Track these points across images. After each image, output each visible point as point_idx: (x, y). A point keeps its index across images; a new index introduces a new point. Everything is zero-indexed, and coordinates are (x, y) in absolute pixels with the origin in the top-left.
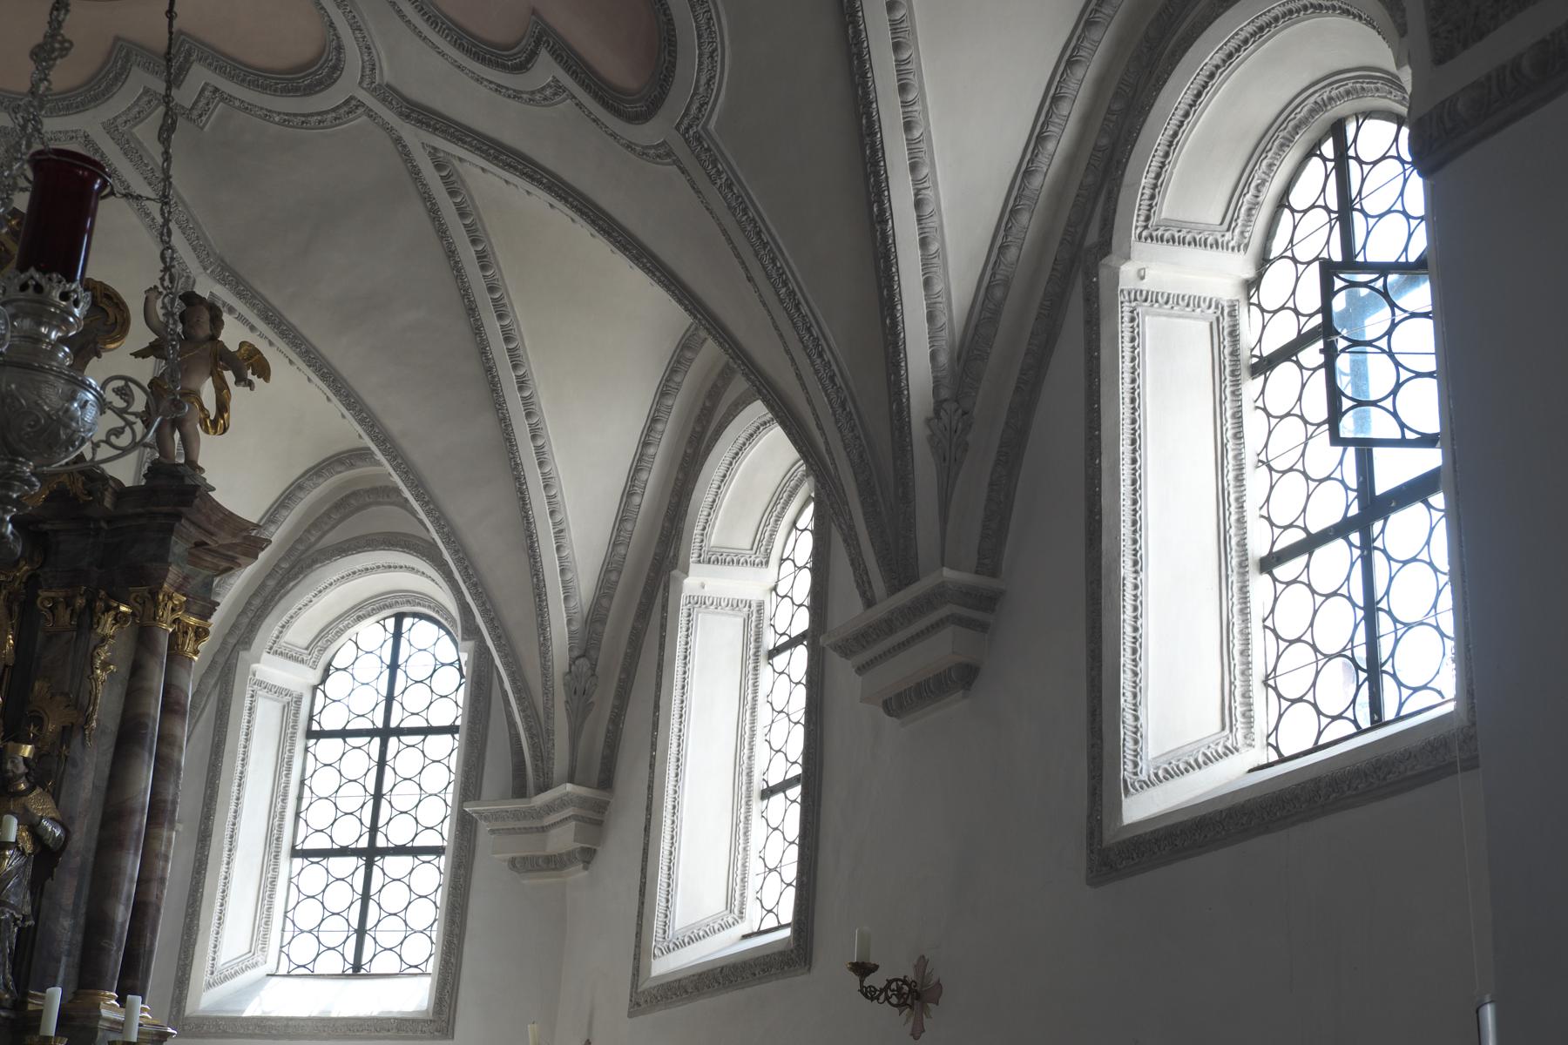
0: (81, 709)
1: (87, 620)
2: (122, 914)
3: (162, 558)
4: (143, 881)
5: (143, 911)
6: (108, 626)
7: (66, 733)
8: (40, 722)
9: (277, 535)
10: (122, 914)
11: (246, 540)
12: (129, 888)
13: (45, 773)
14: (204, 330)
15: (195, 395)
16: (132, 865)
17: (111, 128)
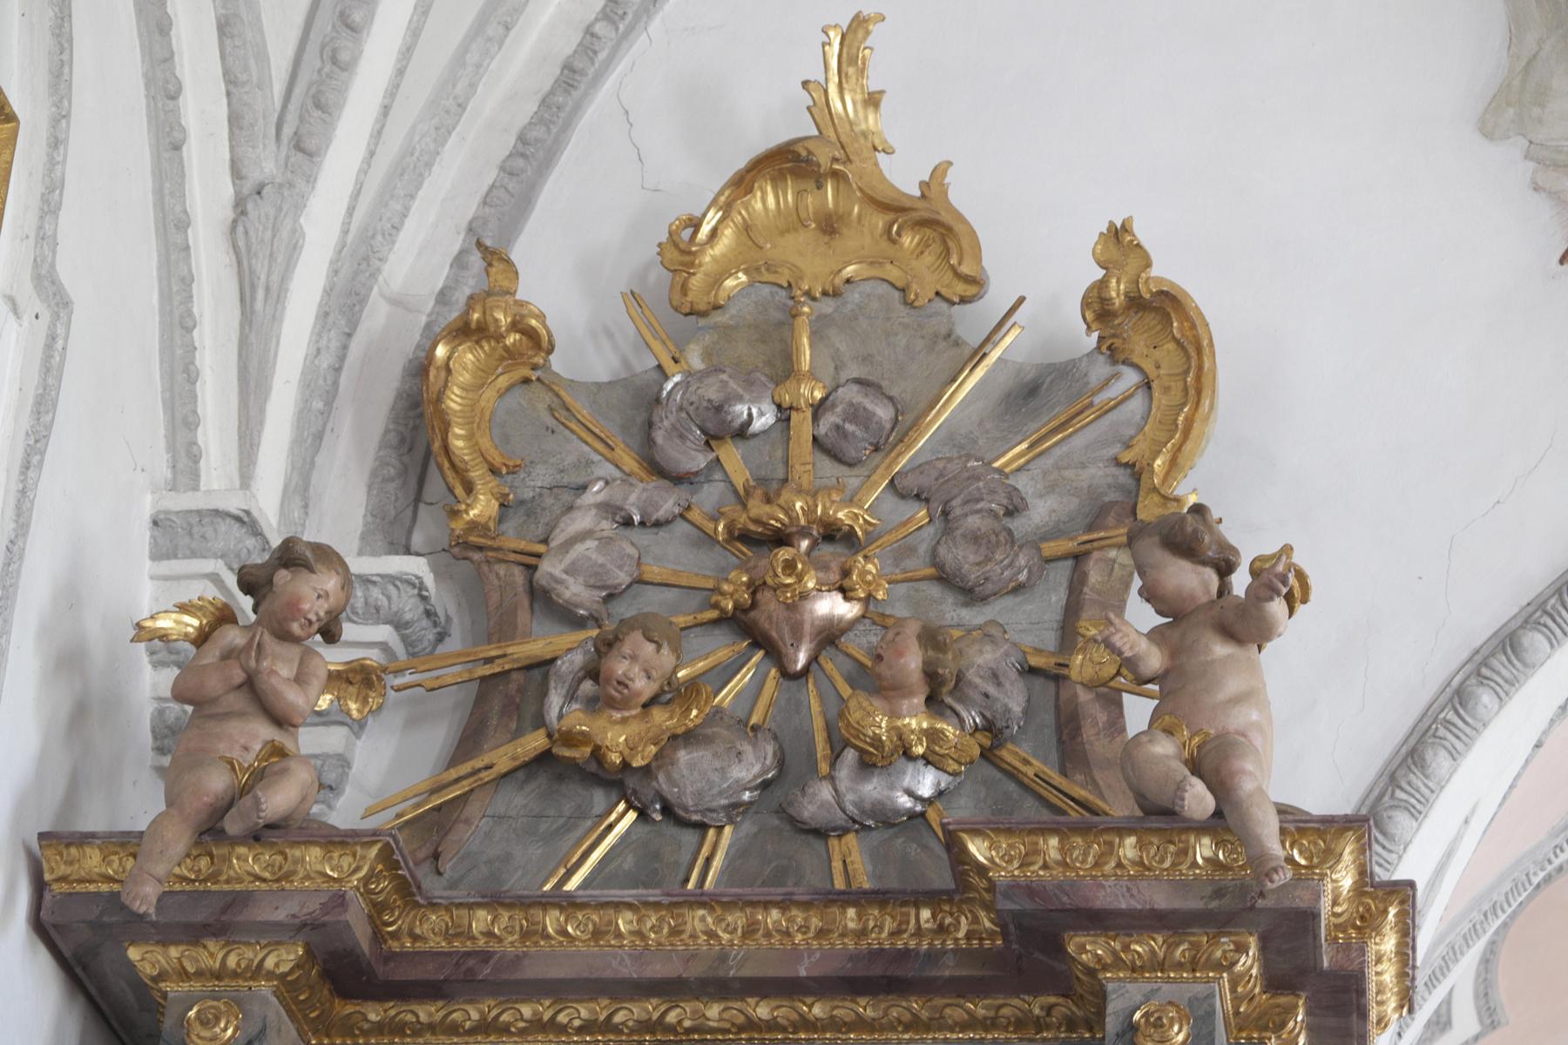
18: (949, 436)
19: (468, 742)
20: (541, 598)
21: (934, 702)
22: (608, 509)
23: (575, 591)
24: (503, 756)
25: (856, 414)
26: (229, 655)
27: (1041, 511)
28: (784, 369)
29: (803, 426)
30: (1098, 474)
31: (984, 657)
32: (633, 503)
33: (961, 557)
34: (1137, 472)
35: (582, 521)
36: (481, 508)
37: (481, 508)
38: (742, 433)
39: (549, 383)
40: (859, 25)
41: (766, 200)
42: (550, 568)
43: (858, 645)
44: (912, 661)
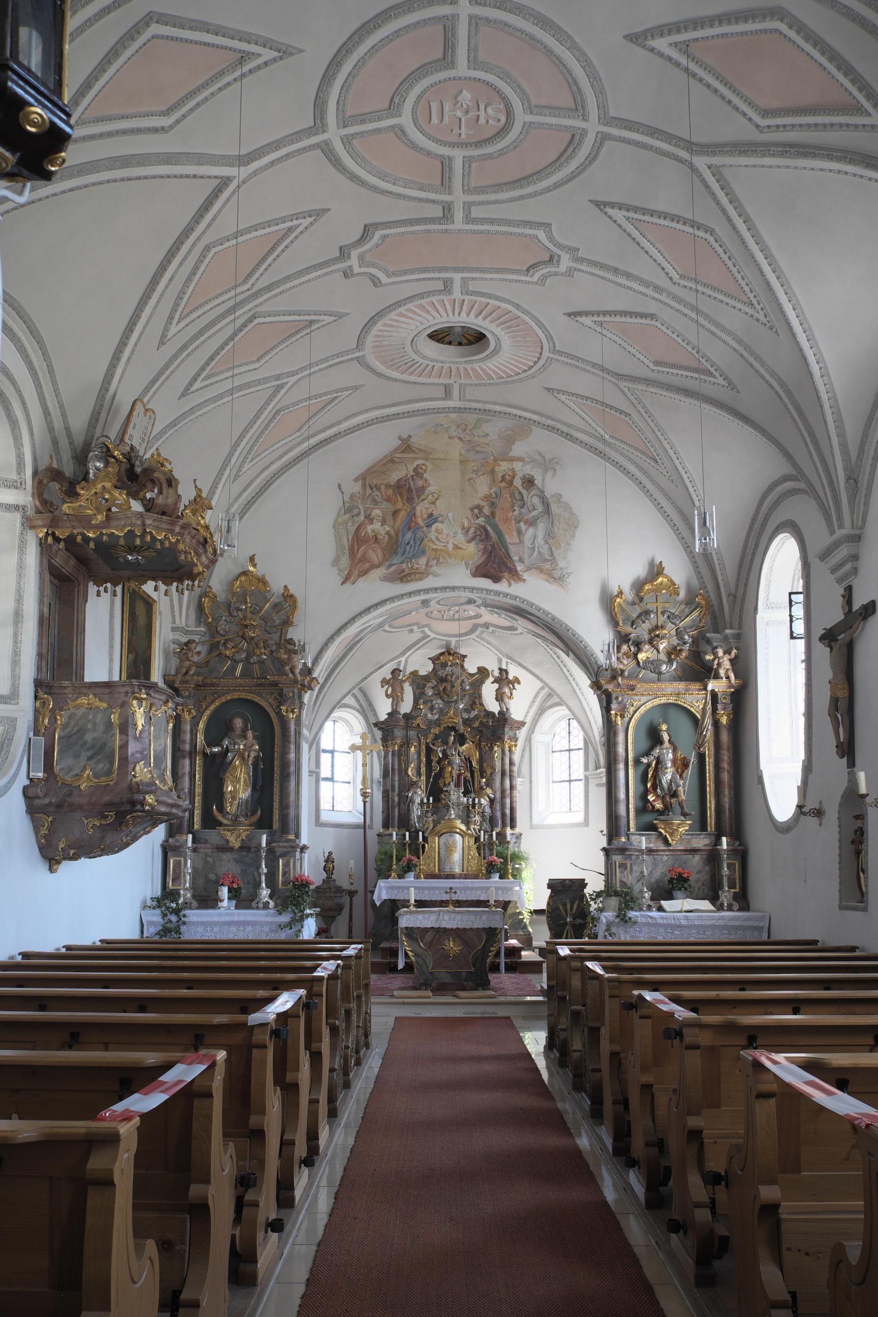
0: (493, 768)
1: (491, 748)
2: (508, 812)
3: (503, 734)
4: (511, 803)
5: (512, 809)
6: (496, 748)
7: (491, 774)
8: (486, 772)
9: (528, 720)
10: (508, 812)
11: (523, 724)
12: (508, 806)
13: (488, 784)
14: (505, 676)
15: (504, 693)
16: (508, 801)
17: (477, 636)
18: (266, 611)
19: (210, 651)
20: (218, 632)
21: (265, 648)
22: (226, 621)
23: (222, 632)
24: (214, 654)
25: (255, 609)
26: (185, 654)
27: (277, 622)
28: (246, 603)
29: (248, 610)
30: (284, 617)
31: (271, 642)
32: (228, 619)
33: (268, 628)
34: (289, 618)
35: (222, 622)
36: (210, 620)
37: (210, 620)
38: (241, 610)
39: (217, 602)
40: (254, 555)
41: (243, 578)
42: (219, 629)
43: (256, 639)
44: (262, 645)
